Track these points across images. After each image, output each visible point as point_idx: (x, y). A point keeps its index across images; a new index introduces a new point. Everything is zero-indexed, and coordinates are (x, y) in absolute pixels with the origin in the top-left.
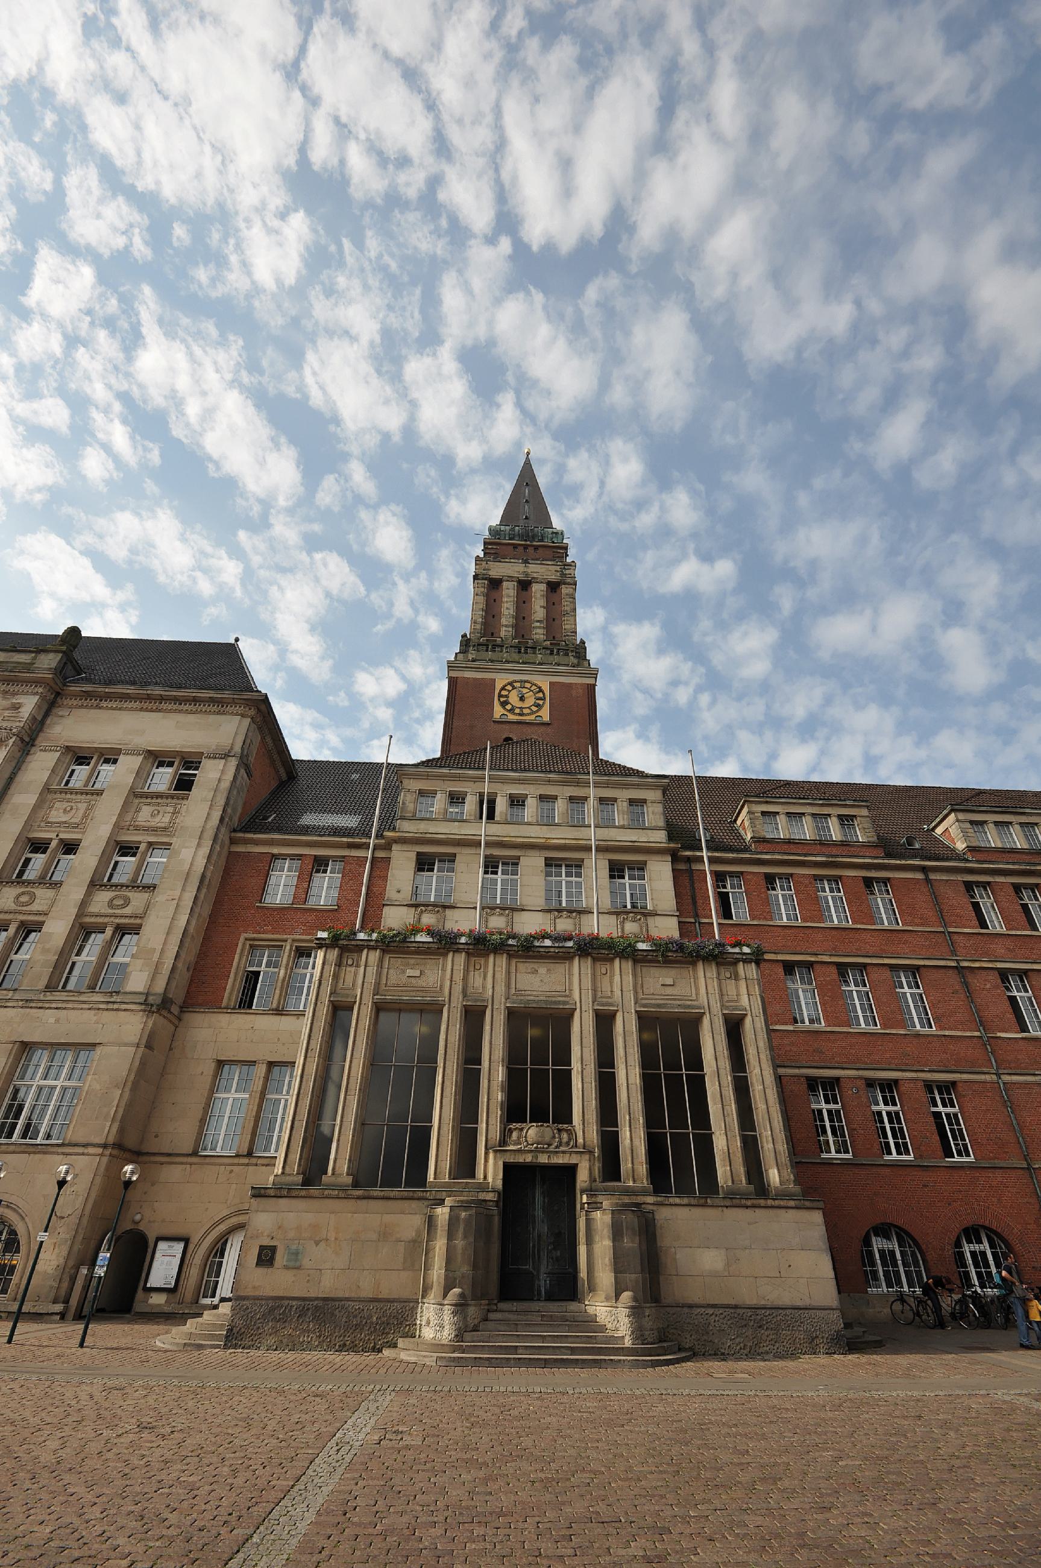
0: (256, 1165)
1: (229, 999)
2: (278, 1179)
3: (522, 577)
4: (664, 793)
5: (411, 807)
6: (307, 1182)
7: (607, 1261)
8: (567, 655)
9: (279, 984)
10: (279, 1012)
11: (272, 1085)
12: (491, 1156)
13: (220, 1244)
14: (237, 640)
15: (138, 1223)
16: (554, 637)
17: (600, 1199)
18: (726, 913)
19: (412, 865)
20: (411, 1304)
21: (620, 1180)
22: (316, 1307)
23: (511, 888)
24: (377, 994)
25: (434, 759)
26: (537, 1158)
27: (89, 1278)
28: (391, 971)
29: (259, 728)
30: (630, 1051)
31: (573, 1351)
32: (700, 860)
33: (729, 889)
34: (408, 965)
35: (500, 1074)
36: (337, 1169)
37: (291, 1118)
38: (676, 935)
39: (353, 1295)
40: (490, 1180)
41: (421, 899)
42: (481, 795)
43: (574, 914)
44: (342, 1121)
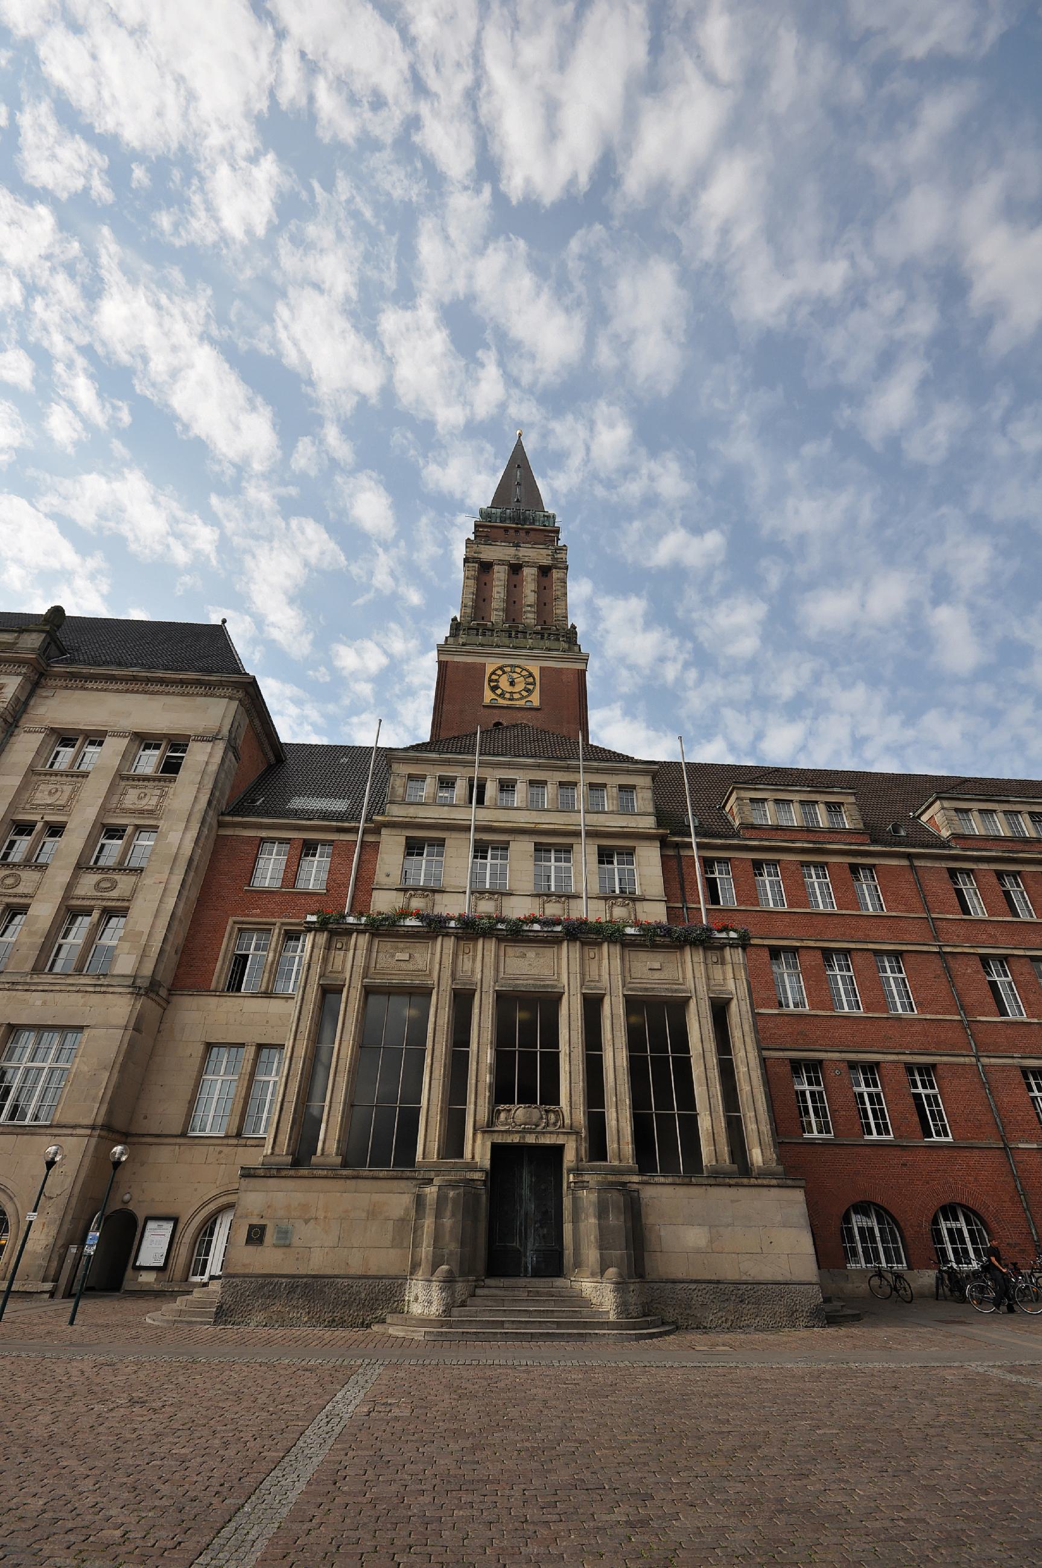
0: (246, 1146)
1: (218, 982)
2: (267, 1160)
4: (653, 779)
5: (400, 791)
6: (296, 1163)
7: (592, 1237)
8: (558, 640)
9: (268, 967)
10: (268, 994)
11: (261, 1067)
12: (479, 1136)
13: (209, 1223)
14: (224, 621)
15: (127, 1203)
16: (545, 622)
17: (586, 1178)
18: (714, 898)
19: (401, 849)
20: (400, 1281)
21: (605, 1159)
22: (306, 1284)
23: (499, 874)
24: (366, 977)
25: (424, 743)
26: (524, 1138)
27: (78, 1257)
28: (381, 955)
29: (247, 711)
30: (617, 1034)
31: (559, 1325)
32: (689, 845)
33: (716, 875)
34: (397, 948)
35: (489, 1057)
36: (326, 1149)
37: (280, 1099)
38: (664, 920)
39: (342, 1272)
40: (477, 1159)
41: (411, 883)
42: (471, 780)
43: (563, 899)
44: (331, 1102)
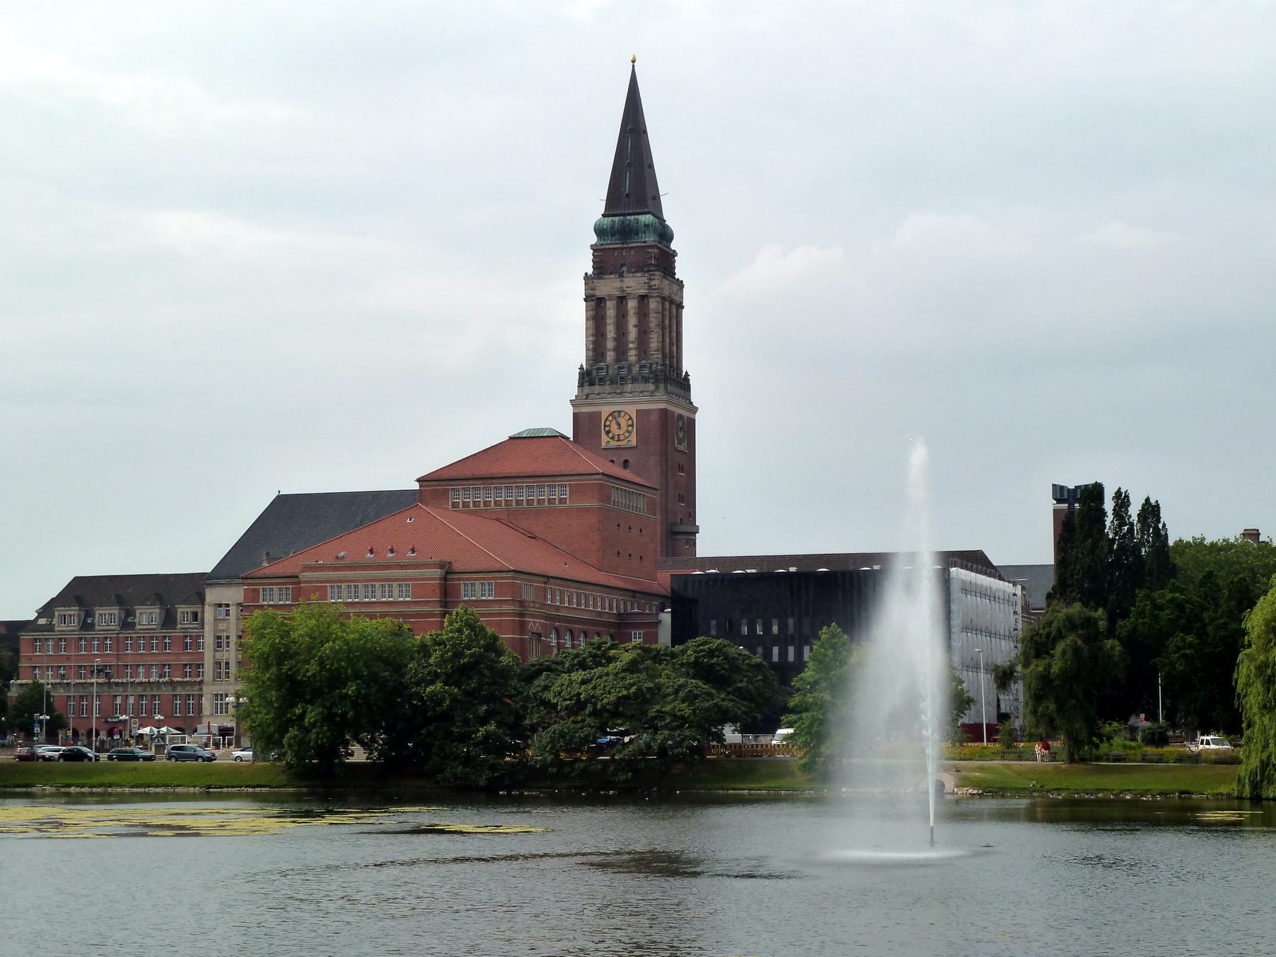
3: (618, 294)
